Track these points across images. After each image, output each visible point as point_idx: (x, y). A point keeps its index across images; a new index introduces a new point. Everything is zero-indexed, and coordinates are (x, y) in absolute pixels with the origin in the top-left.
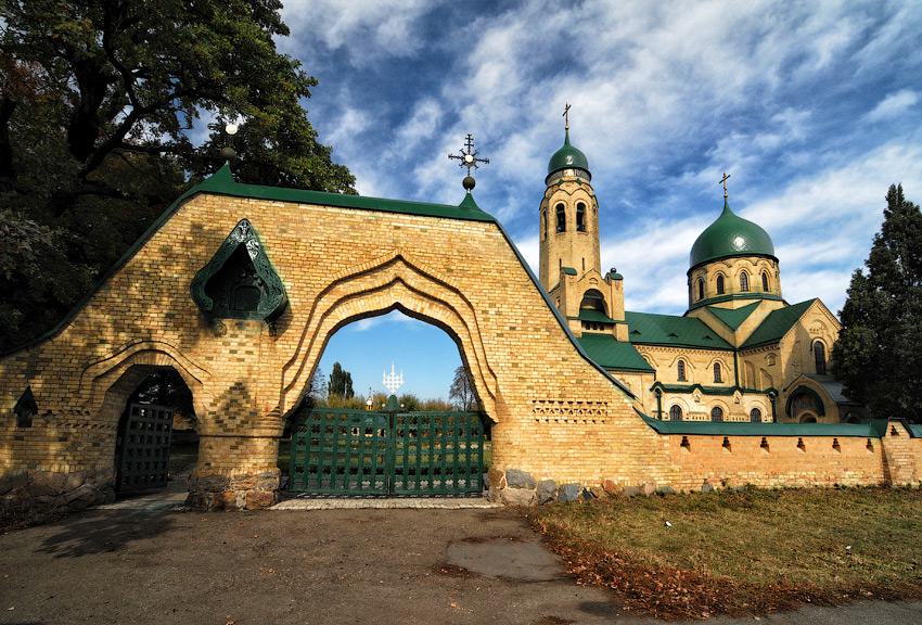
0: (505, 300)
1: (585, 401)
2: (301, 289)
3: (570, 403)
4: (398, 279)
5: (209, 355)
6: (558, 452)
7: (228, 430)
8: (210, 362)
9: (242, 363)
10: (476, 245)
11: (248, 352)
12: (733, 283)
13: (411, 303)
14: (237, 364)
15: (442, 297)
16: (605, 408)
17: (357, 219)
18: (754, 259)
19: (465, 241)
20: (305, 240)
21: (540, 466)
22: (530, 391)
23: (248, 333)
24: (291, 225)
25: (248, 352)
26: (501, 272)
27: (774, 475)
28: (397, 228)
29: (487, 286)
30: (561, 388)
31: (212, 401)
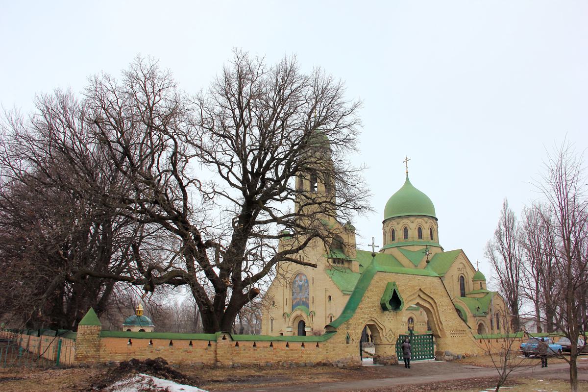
4: (419, 295)
12: (413, 233)
15: (428, 300)
17: (410, 277)
18: (426, 219)
28: (419, 280)
30: (456, 327)
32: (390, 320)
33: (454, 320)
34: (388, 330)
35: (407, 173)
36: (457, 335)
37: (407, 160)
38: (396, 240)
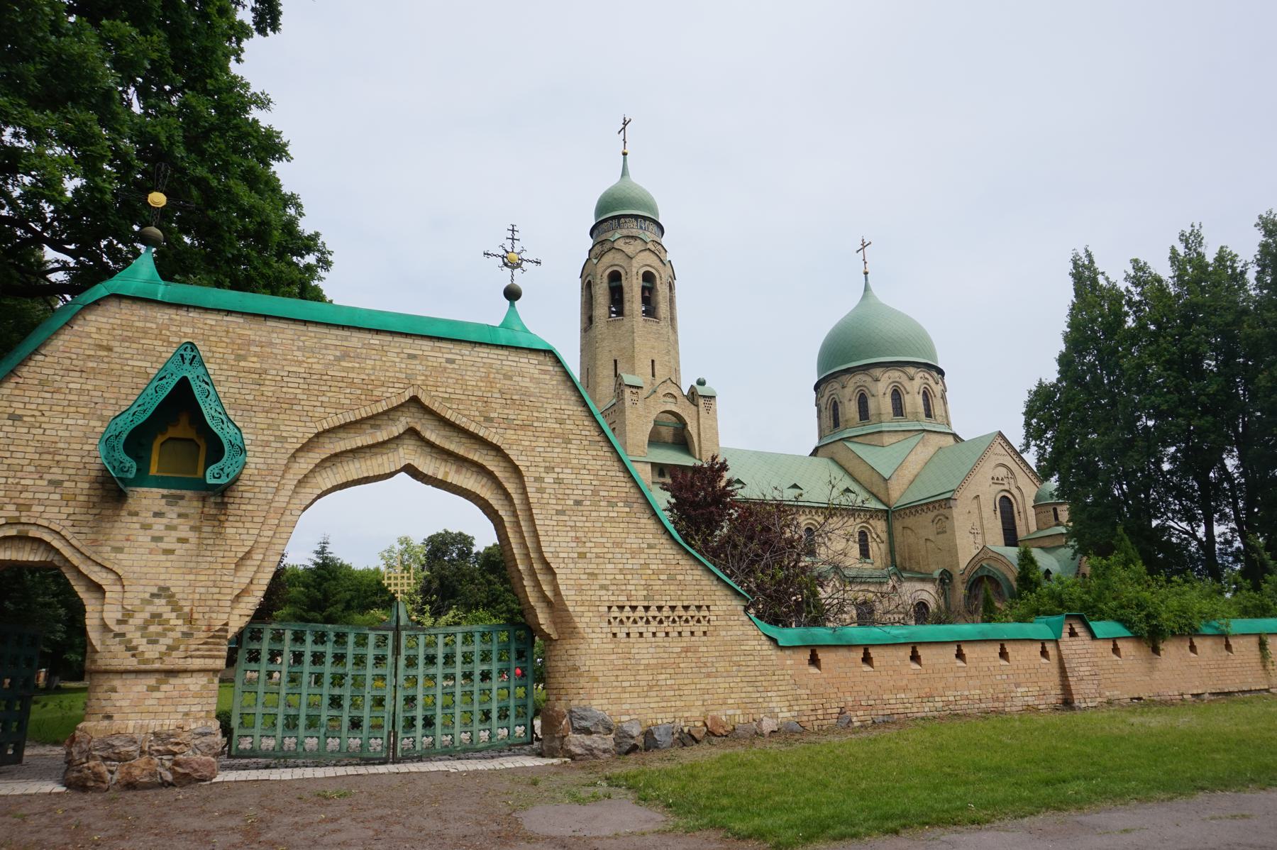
0: (567, 463)
1: (679, 604)
2: (267, 444)
3: (660, 608)
4: (412, 432)
5: (119, 544)
6: (645, 677)
7: (146, 661)
8: (120, 556)
9: (171, 557)
10: (526, 383)
11: (183, 540)
13: (427, 465)
14: (163, 558)
15: (475, 457)
16: (706, 613)
18: (911, 370)
19: (510, 378)
20: (274, 372)
21: (618, 701)
22: (603, 592)
23: (182, 511)
24: (253, 349)
25: (183, 540)
26: (561, 422)
27: (930, 697)
29: (541, 442)
30: (647, 587)
31: (119, 616)
32: (170, 542)
33: (634, 554)
34: (136, 594)
35: (866, 273)
36: (653, 627)
37: (864, 246)
38: (842, 425)
